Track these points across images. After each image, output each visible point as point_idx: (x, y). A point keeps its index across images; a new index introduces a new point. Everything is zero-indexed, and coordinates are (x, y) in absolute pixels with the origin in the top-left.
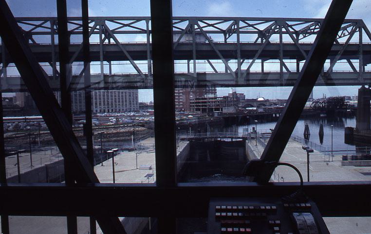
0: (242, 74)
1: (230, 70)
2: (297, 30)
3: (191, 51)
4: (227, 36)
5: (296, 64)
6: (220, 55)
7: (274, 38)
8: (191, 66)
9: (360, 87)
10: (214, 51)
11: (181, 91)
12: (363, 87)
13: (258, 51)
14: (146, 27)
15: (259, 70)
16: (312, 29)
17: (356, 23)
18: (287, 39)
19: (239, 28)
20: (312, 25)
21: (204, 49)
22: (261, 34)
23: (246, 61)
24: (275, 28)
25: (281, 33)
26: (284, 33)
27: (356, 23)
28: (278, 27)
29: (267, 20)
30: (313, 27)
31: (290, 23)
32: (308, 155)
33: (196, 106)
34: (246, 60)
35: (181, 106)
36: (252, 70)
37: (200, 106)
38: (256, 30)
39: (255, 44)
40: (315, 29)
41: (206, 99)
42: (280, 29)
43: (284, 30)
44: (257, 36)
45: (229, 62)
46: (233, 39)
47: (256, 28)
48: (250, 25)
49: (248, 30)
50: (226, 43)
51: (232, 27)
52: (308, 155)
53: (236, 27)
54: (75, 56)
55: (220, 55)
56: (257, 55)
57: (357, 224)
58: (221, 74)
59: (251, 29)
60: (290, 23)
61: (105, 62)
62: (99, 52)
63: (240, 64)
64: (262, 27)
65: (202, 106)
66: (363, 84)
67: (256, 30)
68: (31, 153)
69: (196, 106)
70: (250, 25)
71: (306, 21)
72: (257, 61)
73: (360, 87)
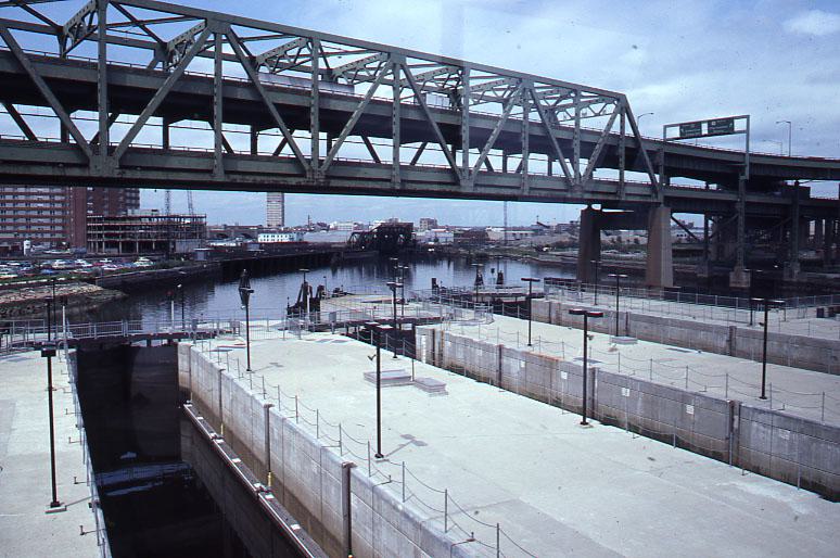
0: (111, 149)
1: (78, 136)
2: (254, 54)
3: (93, 87)
4: (69, 44)
5: (161, 128)
6: (46, 91)
7: (201, 66)
8: (323, 145)
9: (585, 207)
10: (24, 77)
11: (57, 198)
12: (590, 207)
13: (352, 113)
14: (248, 47)
15: (158, 143)
16: (372, 69)
17: (521, 80)
18: (234, 71)
19: (104, 26)
20: (370, 60)
21: (239, 97)
22: (162, 50)
23: (122, 117)
24: (203, 40)
25: (219, 58)
26: (228, 58)
27: (389, 54)
28: (211, 38)
29: (187, 14)
30: (294, 52)
31: (240, 31)
32: (766, 320)
33: (106, 235)
34: (296, 131)
35: (58, 236)
36: (140, 141)
37: (117, 235)
38: (151, 39)
39: (148, 72)
40: (298, 56)
41: (131, 218)
42: (217, 43)
43: (227, 49)
44: (152, 58)
45: (72, 115)
46: (86, 51)
47: (151, 34)
48: (135, 22)
49: (129, 36)
50: (62, 60)
51: (83, 19)
52: (766, 320)
53: (95, 22)
54: (350, 123)
55: (46, 91)
56: (154, 103)
57: (650, 459)
58: (47, 145)
59: (136, 33)
60: (240, 31)
61: (323, 135)
62: (94, 86)
63: (107, 123)
64: (169, 32)
65: (124, 236)
66: (590, 202)
67: (151, 39)
68: (766, 311)
69: (106, 235)
70: (135, 22)
71: (285, 32)
72: (152, 120)
73: (585, 207)
